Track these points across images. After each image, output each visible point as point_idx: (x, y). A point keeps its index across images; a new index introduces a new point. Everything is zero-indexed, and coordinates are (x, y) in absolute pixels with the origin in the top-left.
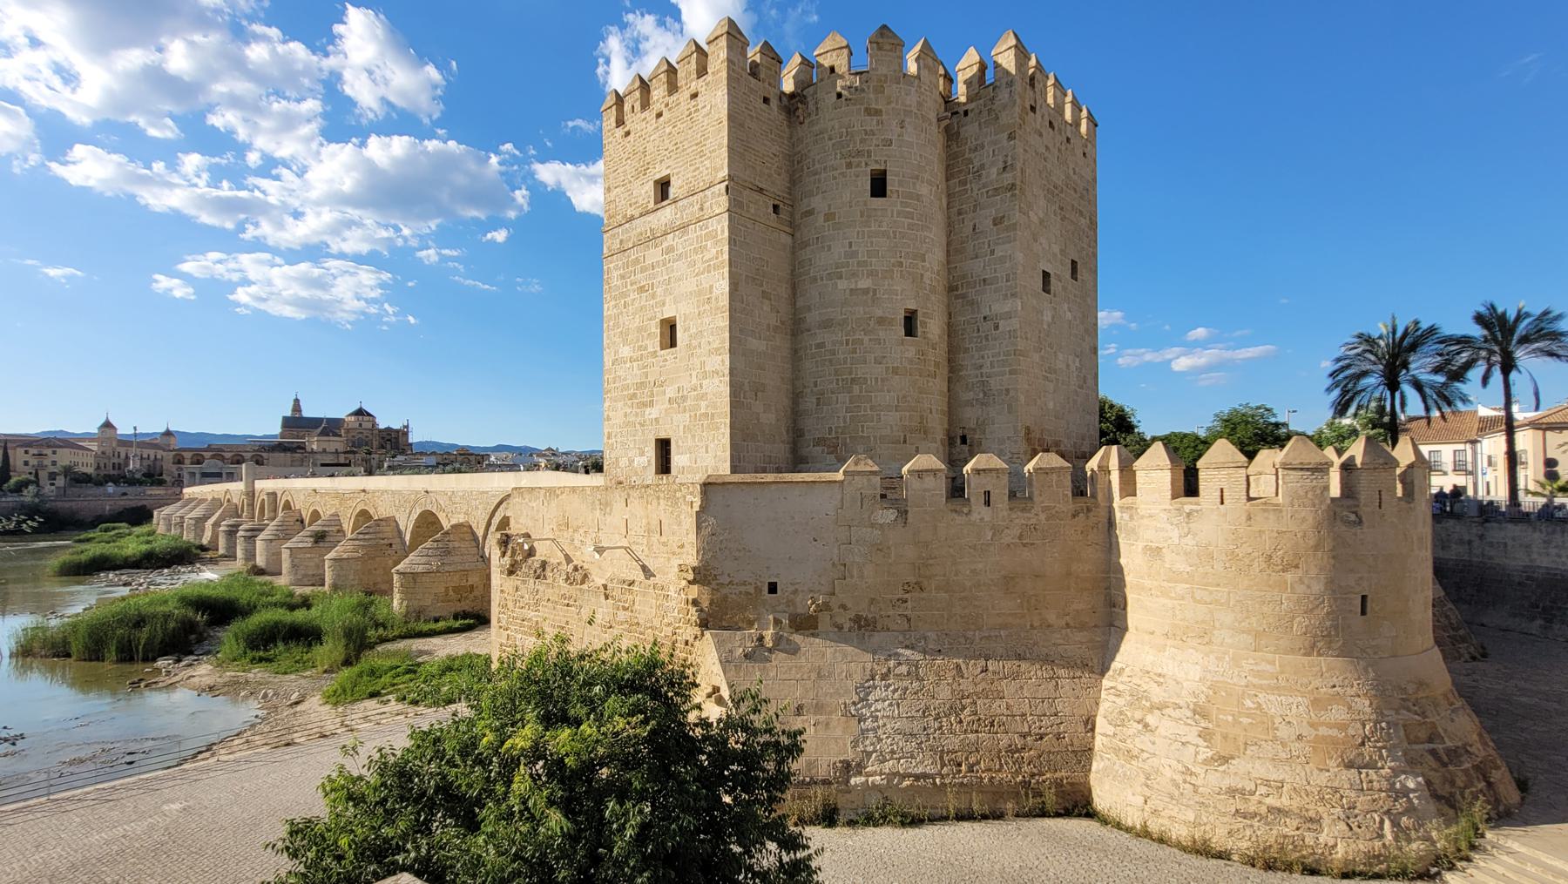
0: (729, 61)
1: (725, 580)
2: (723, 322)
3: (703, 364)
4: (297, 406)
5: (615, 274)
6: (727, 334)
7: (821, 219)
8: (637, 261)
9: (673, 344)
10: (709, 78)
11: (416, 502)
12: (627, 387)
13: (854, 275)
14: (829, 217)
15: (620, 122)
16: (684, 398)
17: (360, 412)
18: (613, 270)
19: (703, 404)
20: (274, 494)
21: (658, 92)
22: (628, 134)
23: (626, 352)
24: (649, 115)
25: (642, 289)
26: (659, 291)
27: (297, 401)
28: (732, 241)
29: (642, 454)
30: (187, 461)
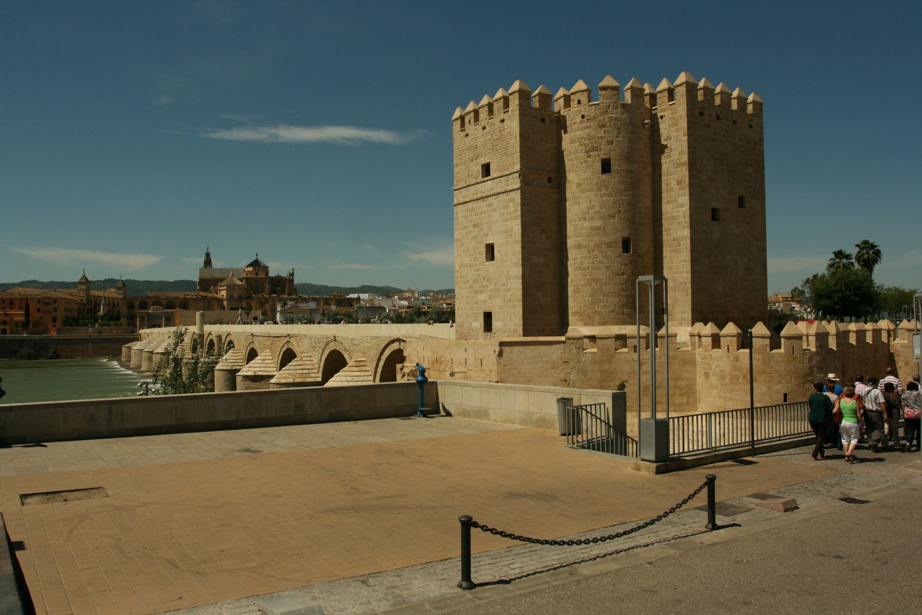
0: (520, 105)
2: (518, 248)
3: (508, 271)
4: (208, 262)
5: (460, 215)
6: (520, 256)
7: (574, 186)
8: (473, 209)
9: (493, 259)
10: (510, 113)
11: (328, 344)
12: (467, 282)
13: (593, 219)
14: (579, 185)
15: (463, 125)
16: (499, 290)
17: (256, 264)
18: (460, 212)
19: (509, 294)
20: (219, 337)
21: (483, 114)
22: (467, 135)
23: (467, 260)
24: (479, 127)
25: (475, 226)
26: (485, 227)
27: (208, 255)
28: (523, 204)
29: (477, 320)
30: (136, 308)
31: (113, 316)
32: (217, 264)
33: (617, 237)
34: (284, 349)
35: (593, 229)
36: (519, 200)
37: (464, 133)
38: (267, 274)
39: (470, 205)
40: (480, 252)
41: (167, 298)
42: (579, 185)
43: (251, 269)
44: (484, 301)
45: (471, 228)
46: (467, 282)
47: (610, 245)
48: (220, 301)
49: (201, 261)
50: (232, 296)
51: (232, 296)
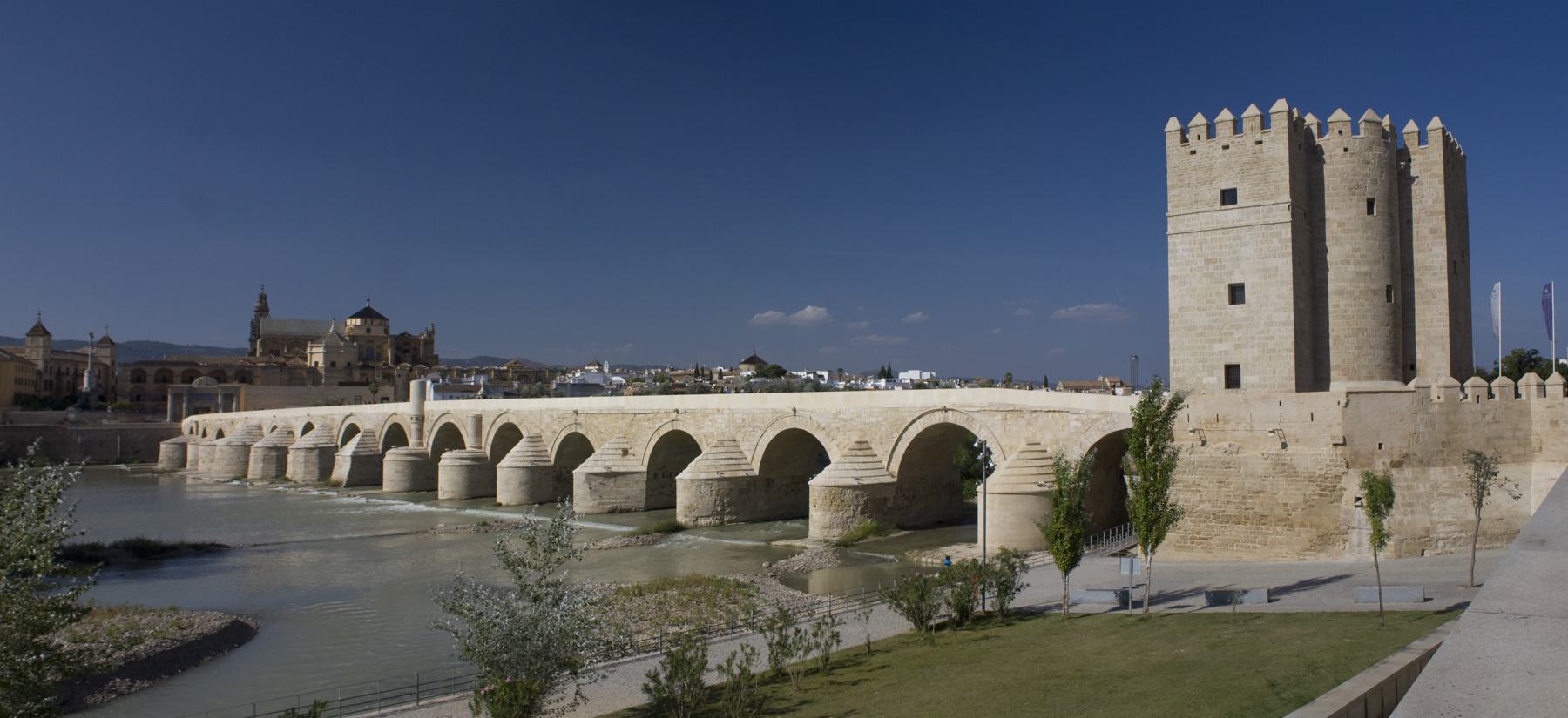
4: (263, 310)
5: (1180, 247)
7: (1335, 226)
12: (1194, 328)
19: (1270, 342)
24: (1216, 144)
27: (263, 298)
29: (1211, 374)
31: (103, 397)
32: (275, 311)
33: (1381, 284)
34: (663, 432)
37: (1188, 150)
39: (1199, 237)
40: (1218, 294)
41: (209, 366)
42: (1341, 224)
44: (1226, 352)
47: (1375, 292)
48: (313, 371)
50: (333, 364)
51: (333, 364)
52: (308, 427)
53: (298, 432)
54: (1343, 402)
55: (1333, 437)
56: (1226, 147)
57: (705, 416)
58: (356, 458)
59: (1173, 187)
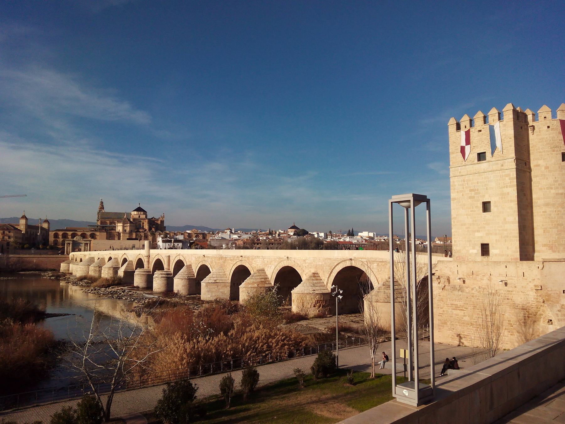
1: (550, 289)
3: (505, 219)
4: (102, 207)
7: (543, 169)
12: (465, 225)
13: (557, 188)
14: (547, 168)
25: (471, 190)
27: (102, 203)
29: (474, 248)
30: (60, 237)
35: (557, 194)
36: (515, 176)
38: (146, 217)
39: (466, 178)
40: (477, 207)
42: (547, 168)
43: (136, 213)
44: (481, 237)
45: (468, 192)
46: (465, 225)
49: (99, 205)
52: (110, 259)
53: (107, 260)
54: (541, 267)
55: (535, 286)
56: (480, 131)
57: (252, 259)
58: (125, 272)
59: (453, 153)
